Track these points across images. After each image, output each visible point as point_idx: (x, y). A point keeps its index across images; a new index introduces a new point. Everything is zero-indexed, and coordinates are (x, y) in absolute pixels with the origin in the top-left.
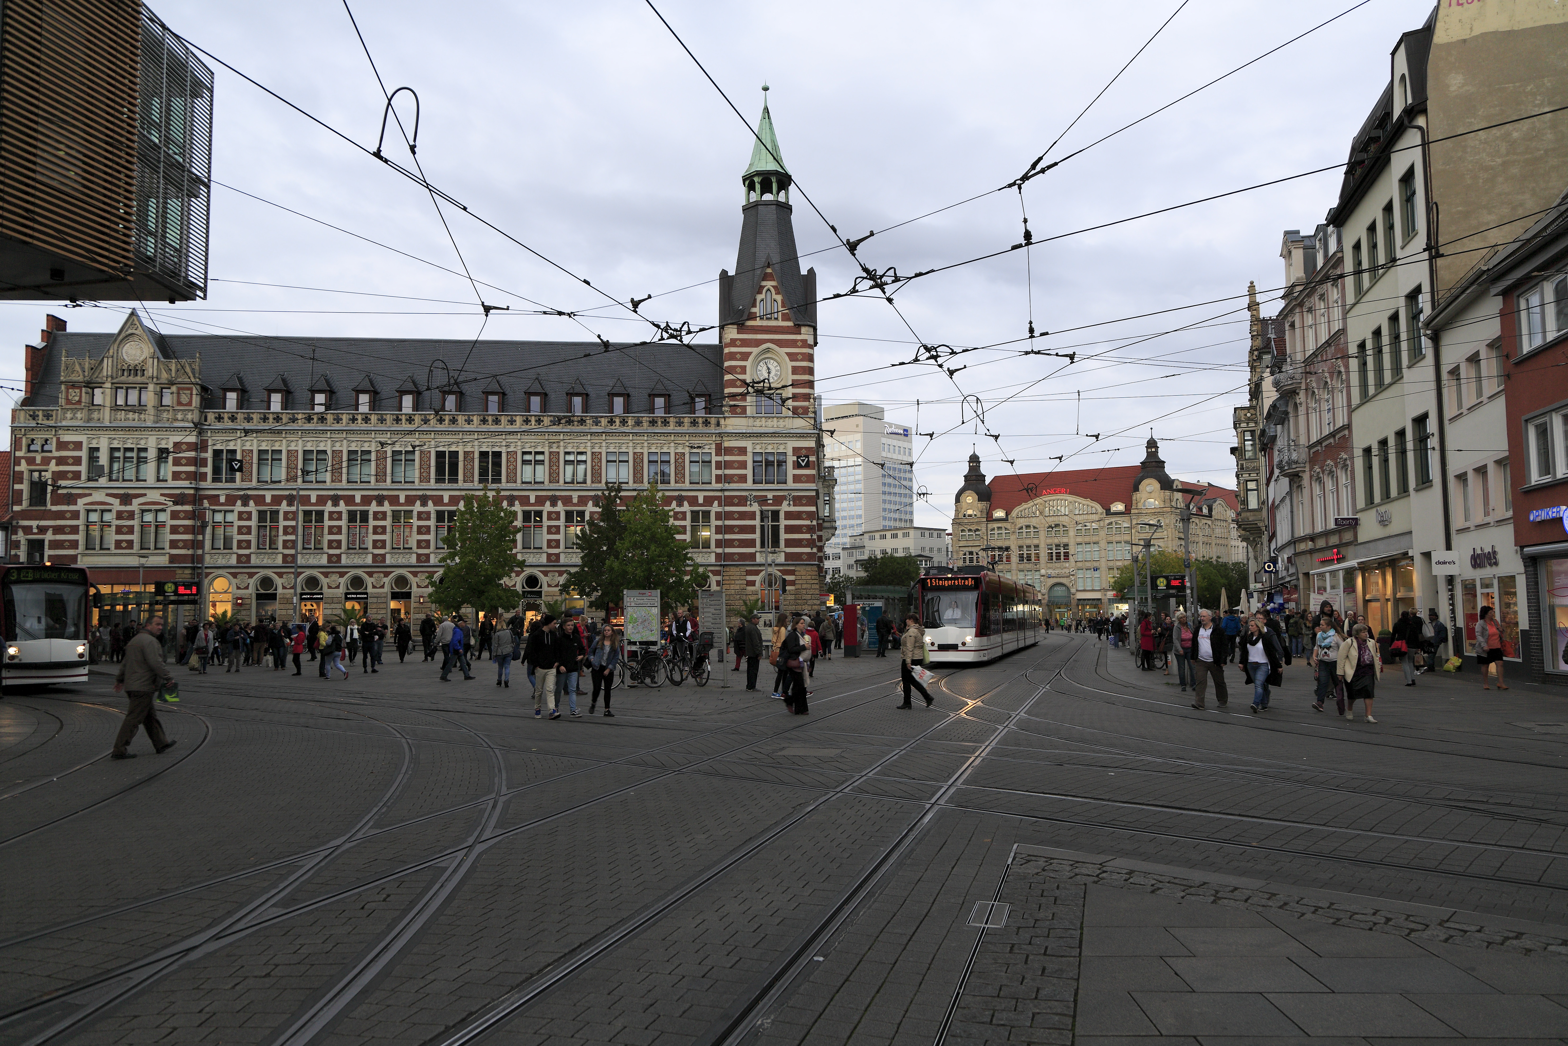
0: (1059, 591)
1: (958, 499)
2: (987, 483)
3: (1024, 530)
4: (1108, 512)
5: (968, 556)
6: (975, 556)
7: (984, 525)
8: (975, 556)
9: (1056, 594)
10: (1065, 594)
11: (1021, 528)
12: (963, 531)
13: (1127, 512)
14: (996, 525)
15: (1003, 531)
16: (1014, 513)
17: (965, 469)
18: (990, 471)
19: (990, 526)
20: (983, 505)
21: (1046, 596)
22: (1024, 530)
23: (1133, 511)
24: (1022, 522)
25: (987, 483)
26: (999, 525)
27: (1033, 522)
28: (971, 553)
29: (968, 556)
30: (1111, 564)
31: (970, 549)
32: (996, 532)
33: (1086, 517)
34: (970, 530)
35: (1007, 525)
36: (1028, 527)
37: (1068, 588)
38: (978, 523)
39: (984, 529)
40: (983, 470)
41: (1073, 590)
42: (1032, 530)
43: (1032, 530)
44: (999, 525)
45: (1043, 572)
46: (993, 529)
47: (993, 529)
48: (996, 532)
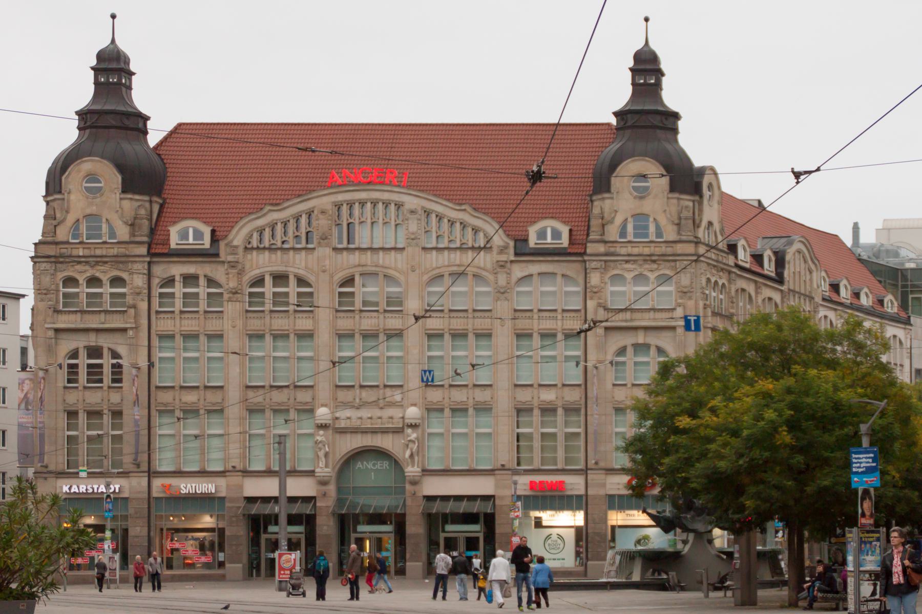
1: (55, 183)
3: (269, 289)
6: (107, 362)
7: (141, 267)
8: (107, 362)
10: (389, 481)
11: (260, 282)
12: (70, 281)
14: (177, 270)
15: (202, 290)
16: (238, 236)
18: (164, 104)
19: (161, 270)
21: (332, 488)
22: (269, 289)
23: (591, 248)
24: (262, 263)
26: (191, 269)
27: (298, 264)
28: (95, 352)
29: (83, 361)
30: (524, 396)
31: (92, 340)
32: (178, 289)
33: (456, 257)
34: (93, 281)
35: (218, 273)
36: (280, 278)
37: (396, 464)
38: (121, 260)
39: (139, 281)
41: (412, 470)
42: (292, 289)
43: (292, 289)
44: (191, 269)
45: (323, 413)
46: (170, 282)
47: (170, 282)
48: (178, 289)
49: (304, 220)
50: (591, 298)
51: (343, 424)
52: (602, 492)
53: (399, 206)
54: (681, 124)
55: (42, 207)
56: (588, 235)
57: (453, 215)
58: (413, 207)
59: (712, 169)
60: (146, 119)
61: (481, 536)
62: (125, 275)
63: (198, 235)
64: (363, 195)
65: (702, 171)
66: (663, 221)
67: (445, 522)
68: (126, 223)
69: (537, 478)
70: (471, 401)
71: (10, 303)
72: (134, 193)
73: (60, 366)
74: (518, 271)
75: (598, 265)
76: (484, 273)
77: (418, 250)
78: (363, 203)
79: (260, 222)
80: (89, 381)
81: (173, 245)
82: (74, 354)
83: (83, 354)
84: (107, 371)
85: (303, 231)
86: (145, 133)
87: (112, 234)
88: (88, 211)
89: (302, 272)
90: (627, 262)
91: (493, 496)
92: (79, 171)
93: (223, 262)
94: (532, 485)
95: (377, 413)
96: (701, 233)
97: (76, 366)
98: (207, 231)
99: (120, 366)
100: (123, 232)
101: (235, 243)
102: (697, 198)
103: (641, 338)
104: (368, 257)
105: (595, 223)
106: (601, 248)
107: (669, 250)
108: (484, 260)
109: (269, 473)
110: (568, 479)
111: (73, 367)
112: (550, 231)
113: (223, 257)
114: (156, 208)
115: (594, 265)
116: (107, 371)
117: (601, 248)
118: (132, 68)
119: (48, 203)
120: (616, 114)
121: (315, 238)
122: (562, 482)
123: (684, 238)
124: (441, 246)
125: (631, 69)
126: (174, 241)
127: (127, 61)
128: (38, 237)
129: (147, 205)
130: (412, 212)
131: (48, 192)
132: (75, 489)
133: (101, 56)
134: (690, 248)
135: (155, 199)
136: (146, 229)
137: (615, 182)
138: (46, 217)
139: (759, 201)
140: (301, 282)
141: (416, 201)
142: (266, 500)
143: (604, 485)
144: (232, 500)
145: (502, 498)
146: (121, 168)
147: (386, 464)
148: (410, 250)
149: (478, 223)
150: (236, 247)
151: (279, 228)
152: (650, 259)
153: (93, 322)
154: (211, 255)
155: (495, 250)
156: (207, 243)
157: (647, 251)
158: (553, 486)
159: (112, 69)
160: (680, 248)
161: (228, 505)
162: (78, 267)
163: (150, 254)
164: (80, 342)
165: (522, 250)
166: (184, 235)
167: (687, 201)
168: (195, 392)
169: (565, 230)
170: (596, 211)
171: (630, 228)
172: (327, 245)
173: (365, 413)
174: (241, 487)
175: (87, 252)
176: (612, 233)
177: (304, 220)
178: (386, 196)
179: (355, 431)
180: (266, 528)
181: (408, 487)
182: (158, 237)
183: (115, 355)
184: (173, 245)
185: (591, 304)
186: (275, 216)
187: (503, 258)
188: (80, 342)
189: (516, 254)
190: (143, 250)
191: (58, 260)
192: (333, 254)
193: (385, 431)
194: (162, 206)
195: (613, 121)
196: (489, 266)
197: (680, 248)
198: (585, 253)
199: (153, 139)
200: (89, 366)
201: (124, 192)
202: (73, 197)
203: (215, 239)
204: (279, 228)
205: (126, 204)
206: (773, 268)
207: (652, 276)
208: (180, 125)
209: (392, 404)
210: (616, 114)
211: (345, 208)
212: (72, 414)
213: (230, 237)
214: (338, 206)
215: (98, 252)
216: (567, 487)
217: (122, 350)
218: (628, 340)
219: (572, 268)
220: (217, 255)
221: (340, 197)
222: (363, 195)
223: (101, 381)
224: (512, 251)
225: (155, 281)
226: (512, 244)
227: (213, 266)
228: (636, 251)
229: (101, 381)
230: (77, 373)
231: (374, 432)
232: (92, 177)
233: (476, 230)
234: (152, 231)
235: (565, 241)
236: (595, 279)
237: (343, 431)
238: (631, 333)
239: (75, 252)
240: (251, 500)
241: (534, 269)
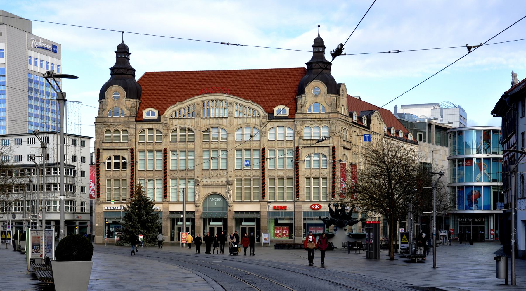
0: (215, 202)
1: (102, 95)
2: (137, 78)
3: (179, 133)
4: (271, 117)
5: (113, 161)
6: (121, 161)
7: (133, 126)
8: (121, 161)
9: (211, 206)
11: (175, 130)
13: (292, 116)
14: (146, 126)
15: (155, 134)
16: (168, 113)
17: (112, 61)
18: (141, 64)
20: (132, 103)
21: (201, 208)
23: (297, 116)
24: (177, 123)
25: (137, 78)
26: (150, 126)
27: (189, 124)
28: (117, 157)
29: (113, 161)
32: (147, 134)
34: (116, 131)
35: (160, 126)
36: (183, 129)
37: (225, 200)
39: (132, 131)
40: (133, 63)
42: (188, 133)
44: (150, 126)
48: (147, 134)
49: (191, 107)
50: (297, 136)
51: (205, 183)
52: (300, 210)
53: (226, 101)
54: (332, 67)
55: (98, 104)
57: (246, 104)
58: (231, 102)
59: (344, 85)
60: (135, 70)
61: (255, 227)
62: (127, 129)
63: (153, 114)
64: (212, 98)
65: (340, 85)
66: (325, 105)
67: (242, 221)
68: (128, 110)
69: (276, 205)
70: (252, 175)
71: (87, 141)
72: (131, 98)
73: (104, 163)
74: (269, 125)
75: (300, 123)
76: (257, 126)
77: (233, 118)
78: (212, 101)
79: (175, 109)
80: (114, 168)
81: (144, 118)
82: (110, 159)
83: (113, 158)
84: (121, 165)
85: (191, 112)
86: (135, 76)
87: (123, 114)
88: (114, 105)
89: (190, 127)
90: (311, 121)
92: (111, 90)
94: (274, 208)
95: (218, 180)
96: (339, 110)
97: (110, 163)
98: (156, 112)
99: (126, 163)
100: (127, 112)
101: (166, 116)
102: (338, 96)
103: (316, 150)
104: (215, 121)
105: (299, 106)
106: (301, 116)
107: (327, 116)
108: (257, 121)
109: (178, 202)
110: (288, 205)
111: (109, 163)
112: (281, 110)
113: (162, 121)
114: (138, 104)
115: (298, 122)
116: (121, 165)
117: (301, 116)
118: (130, 52)
119: (100, 103)
120: (307, 64)
121: (195, 114)
122: (286, 206)
123: (333, 111)
124: (241, 116)
125: (313, 46)
126: (145, 116)
127: (128, 49)
128: (97, 115)
129: (135, 103)
130: (230, 103)
131: (100, 99)
133: (119, 47)
134: (335, 115)
135: (138, 100)
136: (134, 112)
137: (306, 90)
139: (360, 97)
140: (190, 130)
141: (232, 99)
142: (177, 212)
143: (301, 208)
144: (165, 212)
145: (263, 212)
146: (125, 89)
147: (220, 199)
148: (229, 118)
149: (255, 107)
151: (182, 110)
152: (321, 120)
153: (117, 146)
154: (158, 120)
155: (261, 118)
156: (156, 117)
157: (318, 117)
158: (282, 208)
159: (123, 52)
160: (331, 115)
161: (163, 214)
163: (136, 121)
164: (112, 154)
165: (271, 117)
166: (148, 114)
167: (334, 97)
168: (152, 172)
169: (287, 109)
170: (299, 101)
172: (200, 117)
173: (212, 180)
174: (168, 208)
175: (114, 121)
176: (306, 110)
177: (191, 107)
178: (221, 98)
179: (209, 186)
180: (177, 223)
181: (228, 208)
182: (138, 115)
183: (124, 159)
184: (144, 118)
185: (297, 138)
186: (181, 106)
187: (264, 120)
188: (112, 154)
189: (269, 119)
190: (133, 119)
191: (103, 123)
192: (202, 120)
193: (220, 187)
195: (306, 67)
196: (259, 124)
197: (331, 115)
198: (295, 118)
199: (138, 76)
200: (115, 163)
201: (127, 98)
202: (109, 100)
203: (159, 115)
204: (182, 110)
205: (127, 102)
206: (366, 123)
208: (147, 73)
209: (223, 177)
210: (307, 64)
211: (206, 102)
212: (109, 180)
213: (165, 114)
214: (204, 102)
215: (118, 121)
217: (126, 157)
218: (311, 151)
219: (290, 123)
220: (160, 121)
221: (204, 98)
222: (212, 98)
223: (119, 168)
224: (267, 118)
225: (138, 131)
226: (267, 115)
227: (159, 125)
228: (314, 117)
229: (119, 168)
230: (110, 166)
231: (217, 187)
232: (116, 92)
233: (254, 110)
234: (137, 113)
235: (287, 114)
236: (298, 128)
237: (205, 186)
238: (312, 149)
239: (109, 121)
240: (172, 212)
241: (276, 124)
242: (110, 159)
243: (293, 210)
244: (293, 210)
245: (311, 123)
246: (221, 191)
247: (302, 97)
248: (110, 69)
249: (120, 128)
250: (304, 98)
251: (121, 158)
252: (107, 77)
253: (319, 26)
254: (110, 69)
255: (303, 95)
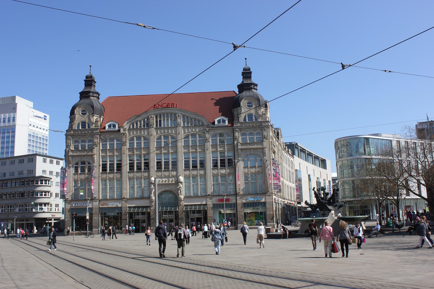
2: (101, 100)
5: (80, 165)
8: (87, 165)
17: (82, 87)
28: (83, 163)
40: (98, 88)
56: (233, 121)
64: (164, 111)
82: (77, 164)
83: (80, 163)
85: (146, 123)
88: (82, 120)
90: (247, 128)
91: (206, 204)
93: (122, 134)
128: (67, 128)
132: (76, 205)
137: (242, 104)
138: (70, 122)
147: (171, 195)
150: (126, 129)
156: (117, 128)
162: (79, 137)
166: (110, 126)
170: (236, 113)
171: (247, 118)
176: (241, 119)
183: (89, 163)
185: (235, 142)
194: (103, 119)
200: (81, 167)
203: (119, 127)
207: (255, 133)
216: (230, 201)
242: (77, 164)
243: (235, 202)
244: (235, 202)
245: (247, 130)
246: (172, 188)
247: (238, 109)
248: (80, 93)
249: (86, 138)
250: (239, 110)
251: (87, 163)
252: (76, 99)
253: (246, 59)
254: (80, 93)
255: (239, 108)
